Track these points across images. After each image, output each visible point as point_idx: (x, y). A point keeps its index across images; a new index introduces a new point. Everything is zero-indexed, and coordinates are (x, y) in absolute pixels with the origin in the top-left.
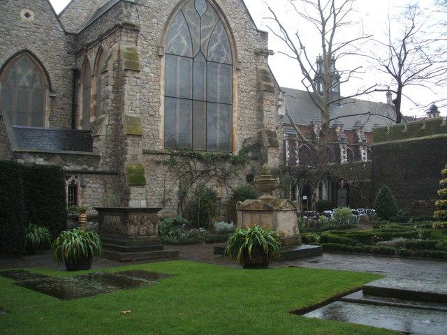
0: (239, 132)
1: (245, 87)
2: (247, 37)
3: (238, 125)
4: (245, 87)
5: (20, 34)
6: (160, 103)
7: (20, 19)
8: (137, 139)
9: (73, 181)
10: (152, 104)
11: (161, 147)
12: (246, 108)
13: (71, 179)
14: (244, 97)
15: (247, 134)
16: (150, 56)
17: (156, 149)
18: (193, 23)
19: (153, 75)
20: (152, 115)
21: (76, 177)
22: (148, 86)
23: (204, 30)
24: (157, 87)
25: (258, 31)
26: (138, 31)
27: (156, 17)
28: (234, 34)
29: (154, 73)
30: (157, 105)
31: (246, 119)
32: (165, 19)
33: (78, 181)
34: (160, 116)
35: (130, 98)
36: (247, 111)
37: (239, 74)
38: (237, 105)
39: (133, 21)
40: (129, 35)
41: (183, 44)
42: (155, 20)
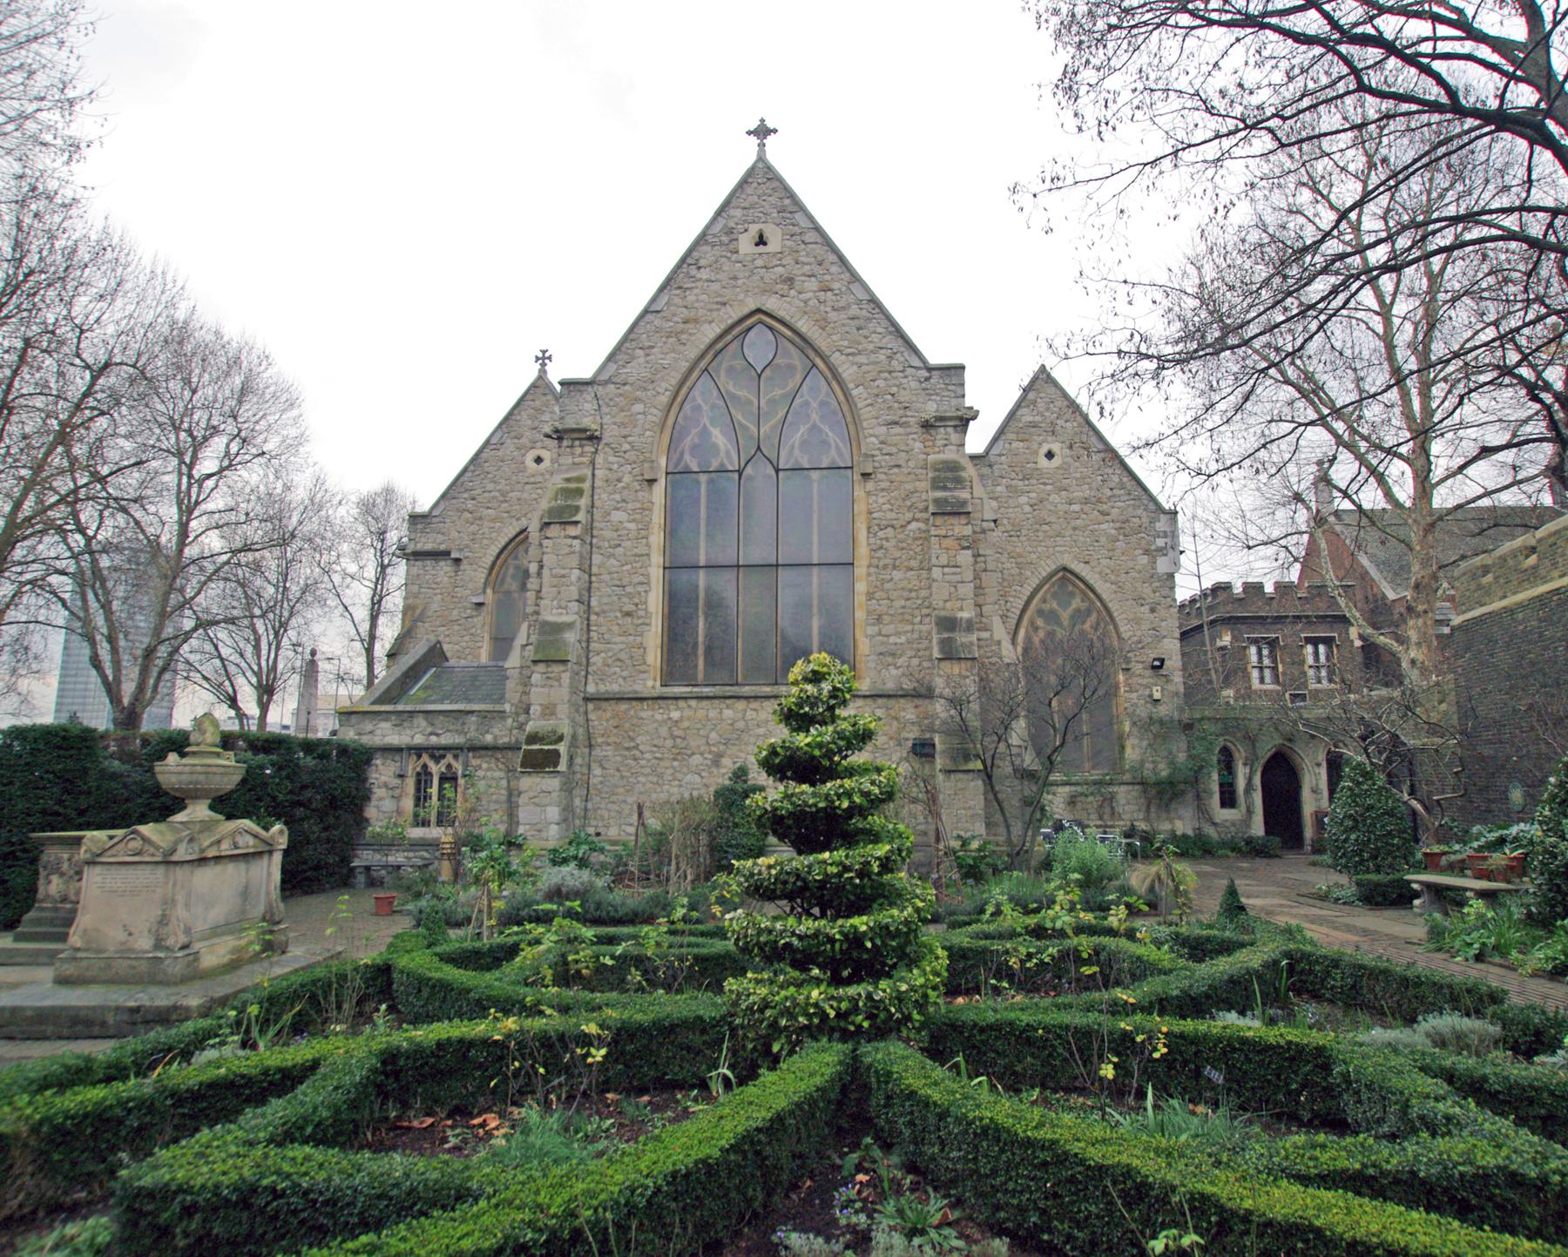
0: (872, 630)
1: (890, 515)
2: (894, 390)
3: (869, 613)
4: (890, 515)
5: (525, 495)
6: (648, 584)
7: (524, 470)
8: (556, 668)
9: (449, 766)
10: (629, 589)
11: (650, 683)
12: (895, 567)
13: (444, 762)
14: (887, 539)
15: (898, 634)
16: (627, 487)
17: (638, 687)
18: (742, 393)
19: (632, 526)
20: (628, 614)
21: (456, 757)
22: (620, 550)
23: (772, 401)
24: (642, 550)
25: (930, 369)
26: (599, 439)
27: (638, 400)
28: (855, 392)
29: (634, 520)
30: (640, 588)
31: (894, 595)
32: (664, 399)
33: (458, 767)
34: (648, 615)
35: (555, 581)
36: (897, 575)
37: (870, 485)
38: (865, 562)
39: (587, 422)
40: (578, 450)
41: (715, 447)
42: (638, 408)
